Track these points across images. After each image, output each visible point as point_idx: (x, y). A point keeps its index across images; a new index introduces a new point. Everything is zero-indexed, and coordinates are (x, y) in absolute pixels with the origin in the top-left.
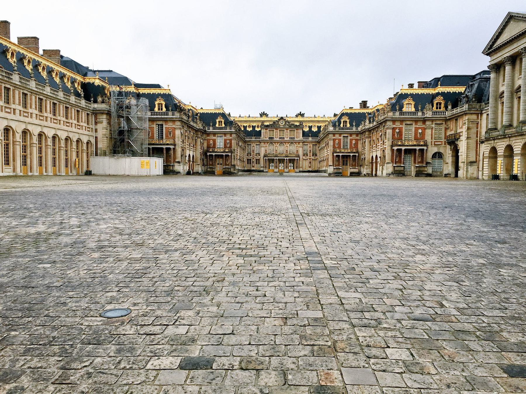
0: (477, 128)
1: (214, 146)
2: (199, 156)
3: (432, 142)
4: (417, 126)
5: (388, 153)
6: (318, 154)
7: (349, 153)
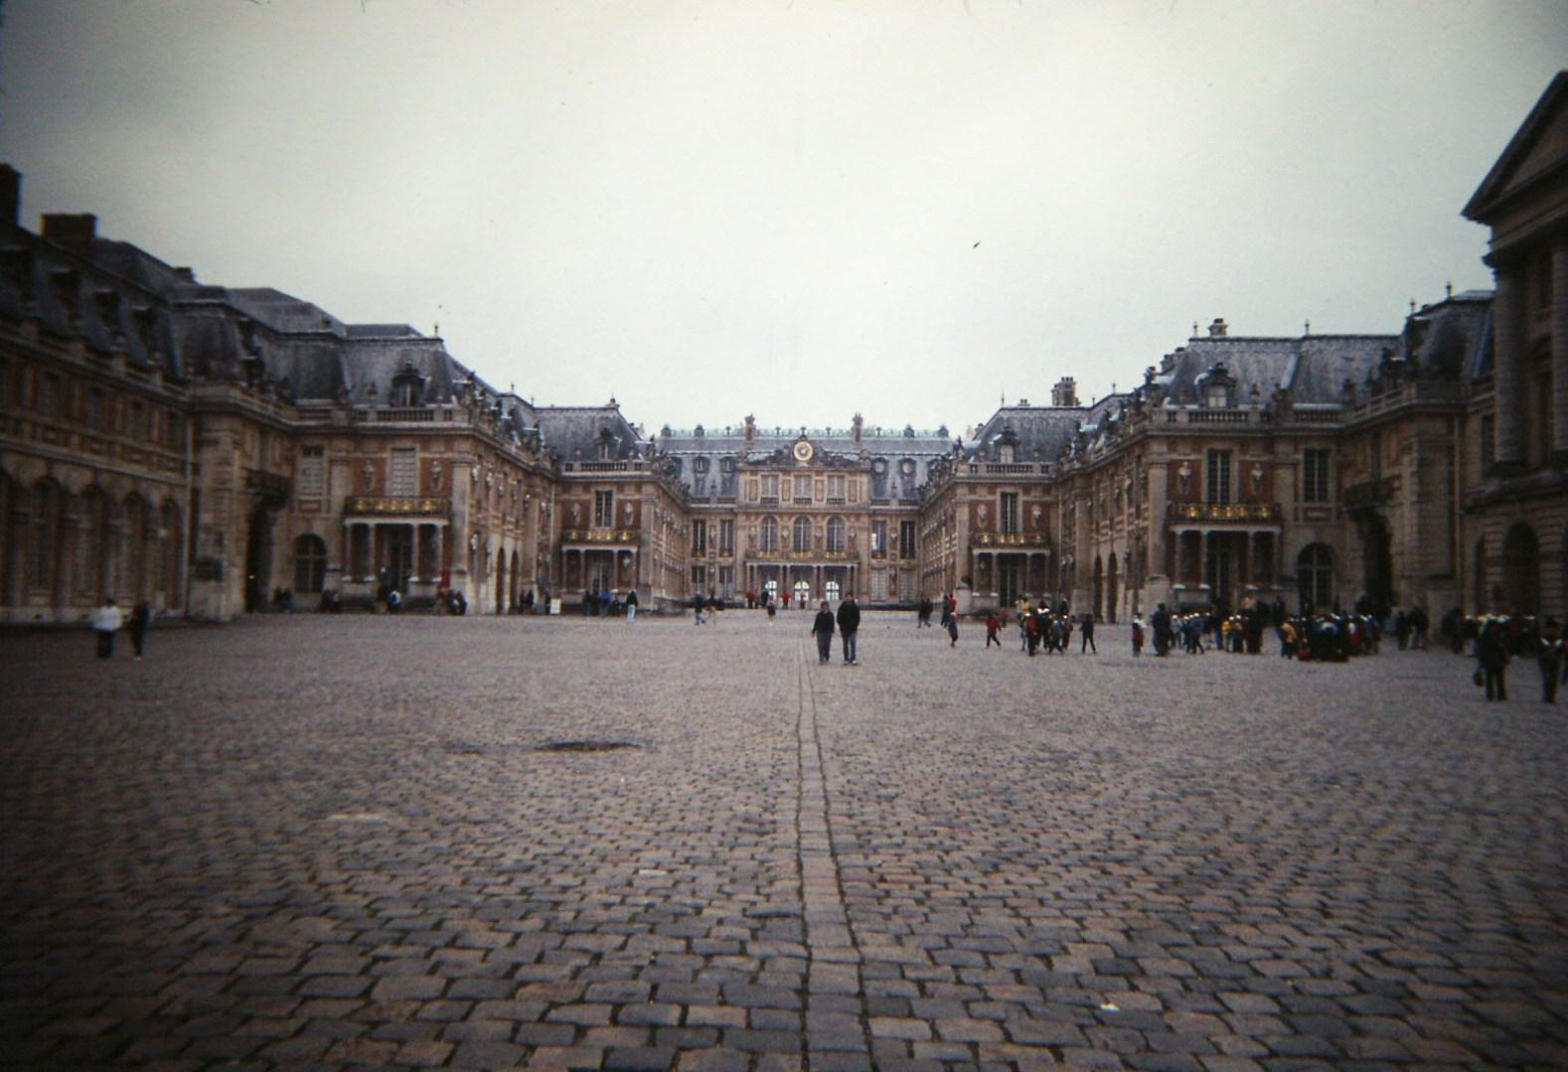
0: (1451, 463)
1: (585, 527)
2: (534, 551)
3: (1296, 509)
4: (1248, 458)
5: (1153, 539)
6: (919, 552)
7: (1021, 546)
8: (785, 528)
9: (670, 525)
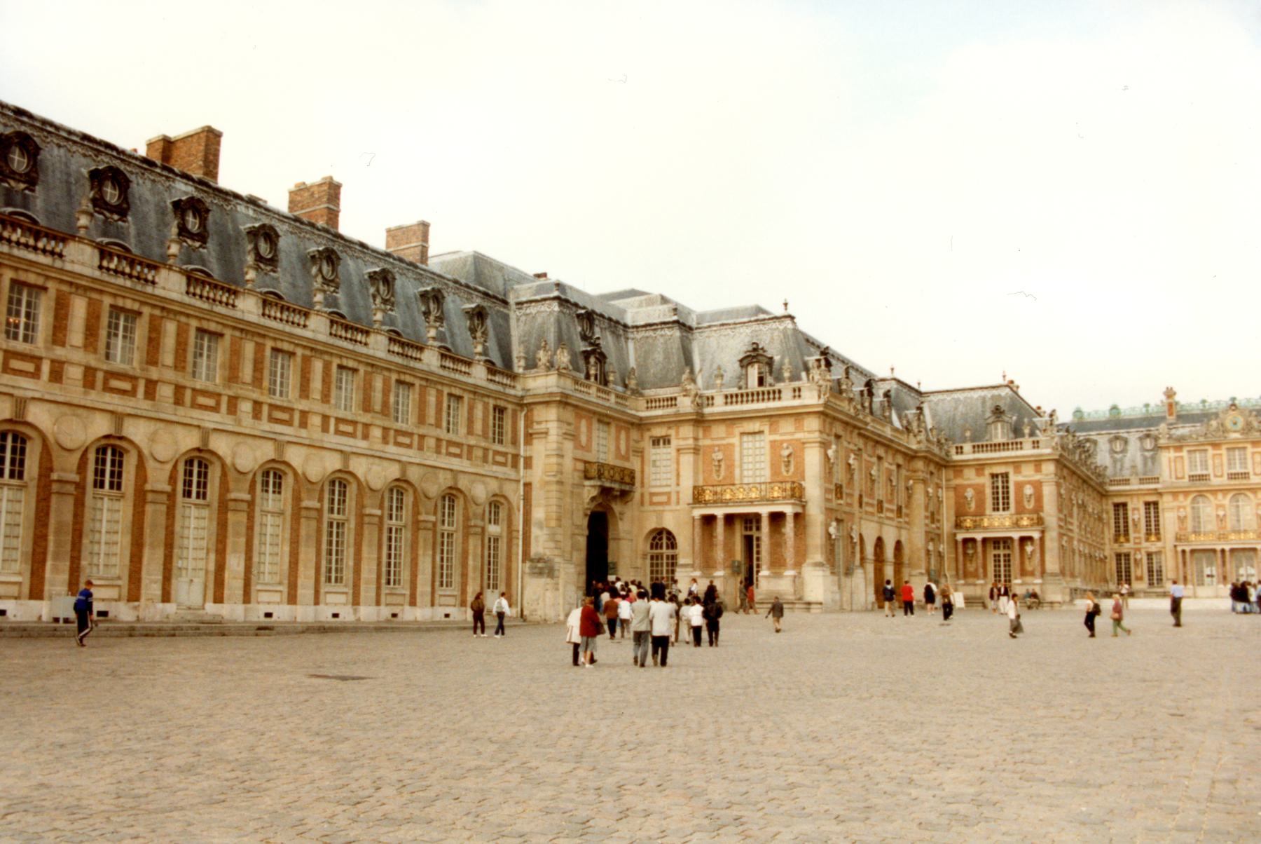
1: (980, 513)
8: (1222, 506)
9: (1083, 506)
